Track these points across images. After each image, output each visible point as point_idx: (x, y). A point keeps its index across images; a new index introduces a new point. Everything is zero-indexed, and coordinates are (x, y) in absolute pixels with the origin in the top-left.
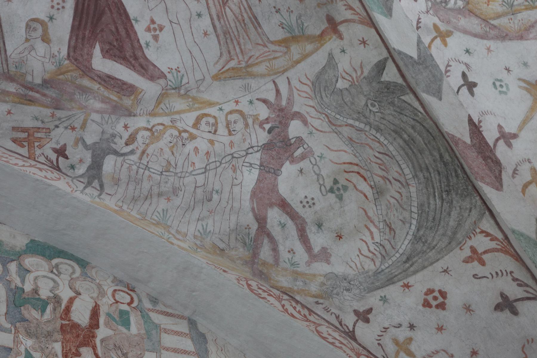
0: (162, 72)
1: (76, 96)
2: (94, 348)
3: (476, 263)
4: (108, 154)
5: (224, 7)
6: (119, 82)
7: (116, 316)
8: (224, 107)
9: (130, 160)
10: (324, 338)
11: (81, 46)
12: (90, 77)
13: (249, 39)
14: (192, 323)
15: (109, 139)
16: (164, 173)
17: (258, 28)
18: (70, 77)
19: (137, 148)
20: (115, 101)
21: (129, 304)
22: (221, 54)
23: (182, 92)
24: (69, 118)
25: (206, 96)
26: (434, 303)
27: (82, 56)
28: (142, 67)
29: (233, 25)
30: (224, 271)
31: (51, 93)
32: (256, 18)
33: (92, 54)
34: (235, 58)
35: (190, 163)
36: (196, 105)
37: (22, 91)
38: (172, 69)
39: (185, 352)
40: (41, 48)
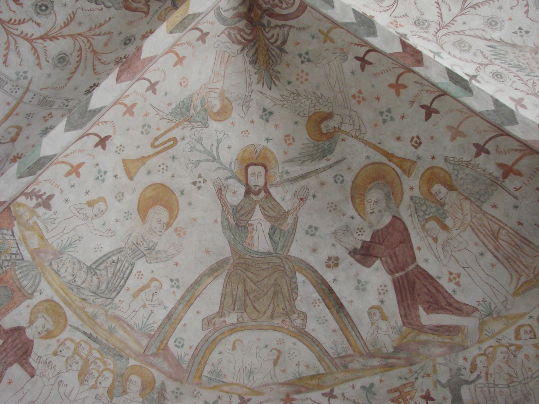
0: (474, 307)
1: (420, 351)
4: (461, 385)
5: (497, 241)
6: (446, 327)
8: (532, 314)
9: (480, 384)
11: (409, 312)
12: (424, 332)
13: (527, 255)
15: (457, 373)
16: (510, 385)
17: (531, 245)
18: (410, 338)
19: (481, 372)
20: (449, 342)
22: (511, 275)
23: (495, 315)
24: (422, 368)
25: (514, 312)
27: (412, 319)
28: (458, 309)
29: (510, 251)
31: (402, 355)
32: (525, 238)
33: (419, 315)
34: (523, 273)
35: (527, 369)
36: (510, 322)
37: (383, 362)
38: (479, 302)
40: (383, 325)
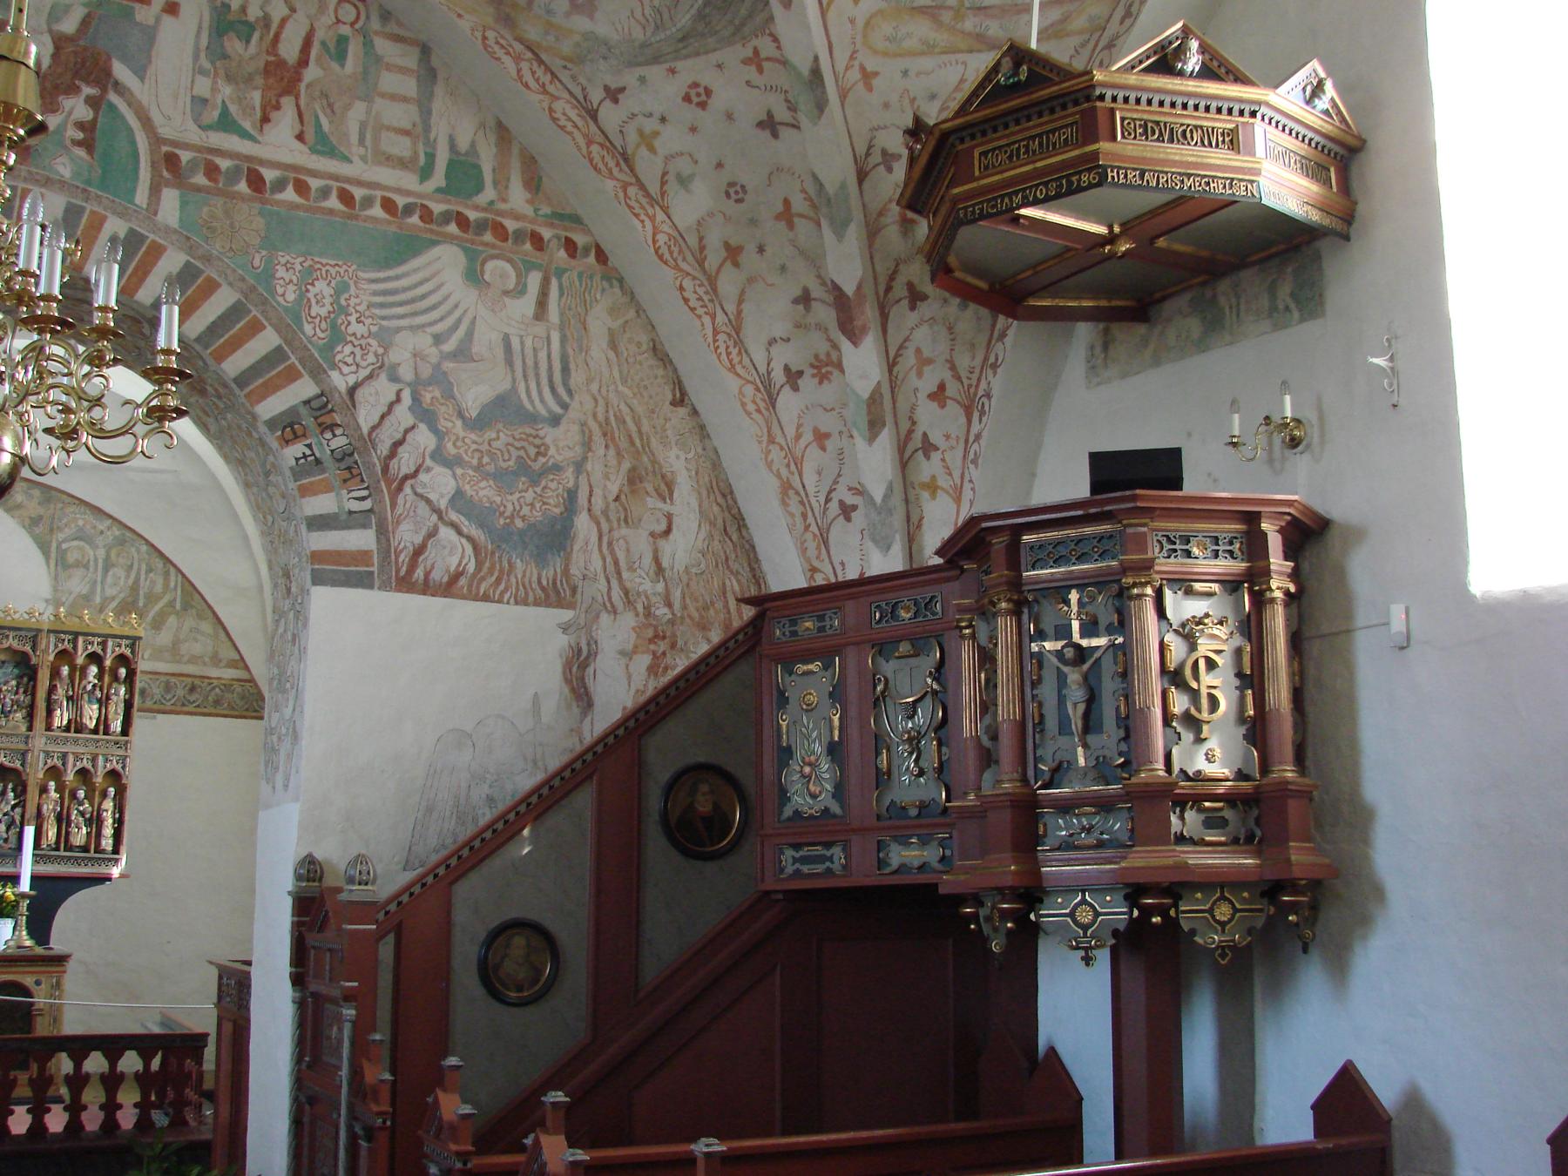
2: (297, 98)
3: (753, 68)
7: (332, 46)
10: (555, 120)
14: (425, 51)
21: (352, 24)
26: (695, 100)
30: (460, 16)
39: (405, 99)
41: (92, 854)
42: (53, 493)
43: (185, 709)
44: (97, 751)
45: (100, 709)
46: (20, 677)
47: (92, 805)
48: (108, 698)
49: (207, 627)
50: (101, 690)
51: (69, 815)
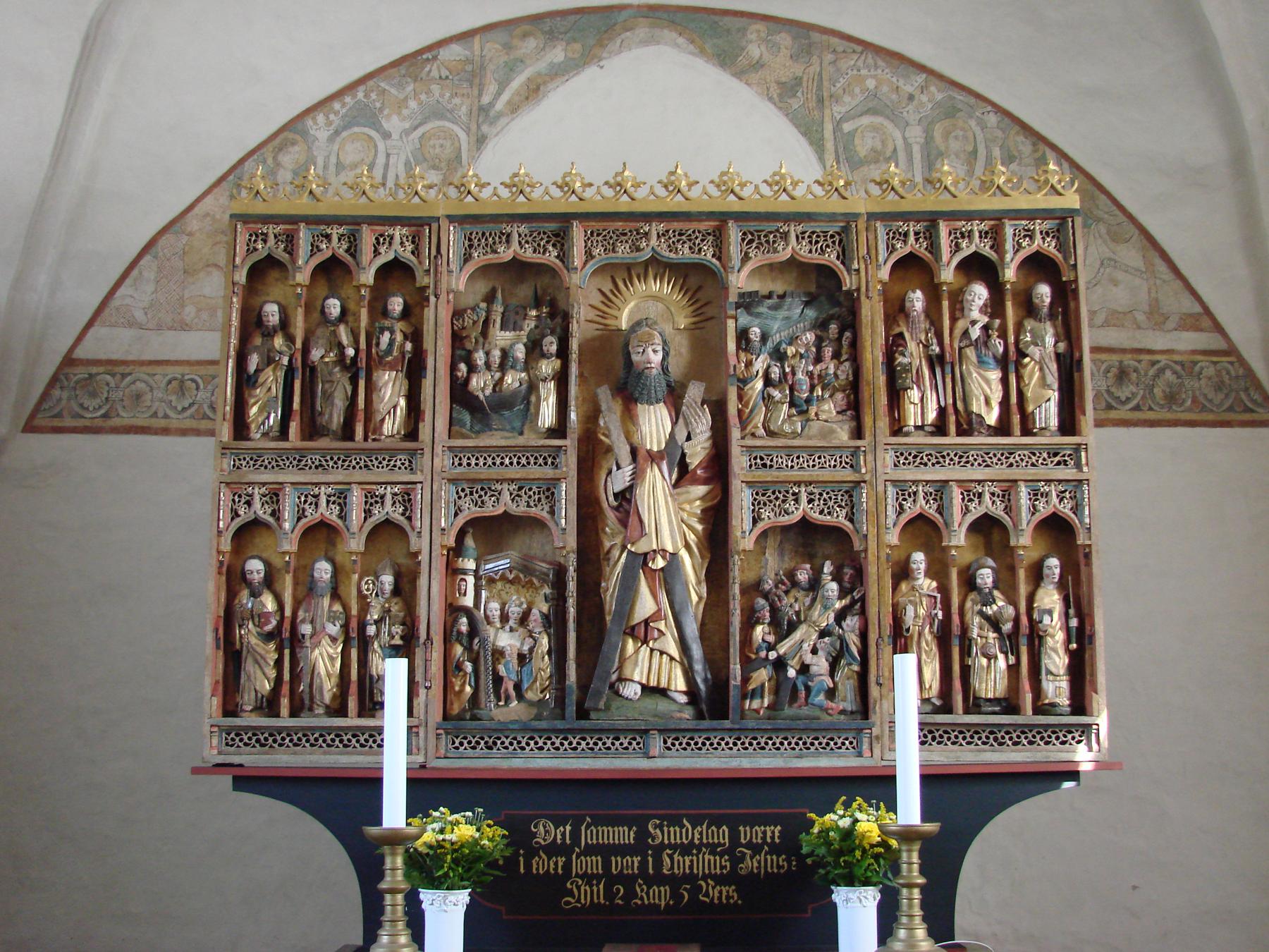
41: (1028, 716)
42: (816, 36)
43: (1113, 415)
44: (1014, 473)
45: (1005, 381)
46: (821, 326)
47: (1012, 601)
48: (1022, 354)
49: (1131, 255)
50: (1003, 335)
51: (965, 629)
